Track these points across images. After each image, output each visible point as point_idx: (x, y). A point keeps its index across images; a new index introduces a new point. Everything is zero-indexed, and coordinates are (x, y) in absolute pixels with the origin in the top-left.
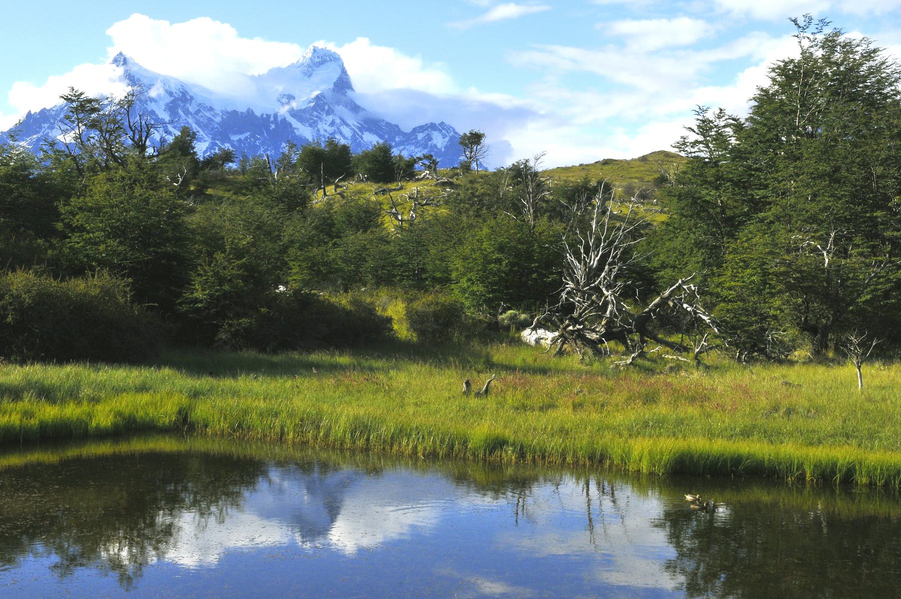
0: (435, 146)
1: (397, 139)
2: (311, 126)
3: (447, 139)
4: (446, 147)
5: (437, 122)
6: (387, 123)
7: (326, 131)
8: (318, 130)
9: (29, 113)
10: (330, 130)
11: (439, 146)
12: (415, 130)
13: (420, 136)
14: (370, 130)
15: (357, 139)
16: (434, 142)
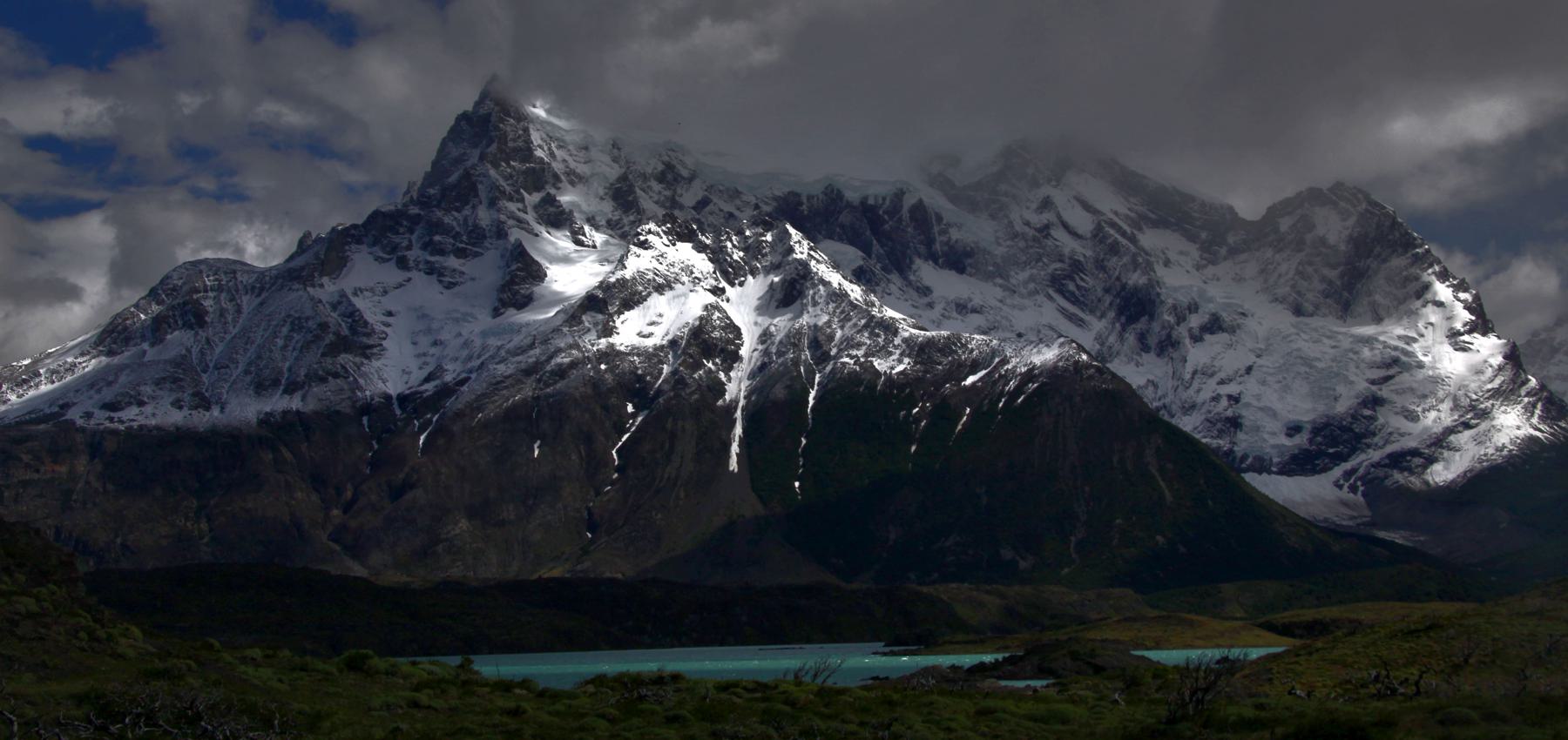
0: (1323, 241)
1: (1231, 239)
2: (993, 217)
3: (1351, 221)
4: (1351, 239)
5: (1325, 183)
6: (1203, 204)
7: (1027, 224)
8: (1011, 224)
9: (307, 235)
10: (1038, 220)
11: (1332, 239)
12: (1274, 213)
13: (1285, 224)
14: (1160, 223)
15: (1105, 237)
16: (1320, 231)
